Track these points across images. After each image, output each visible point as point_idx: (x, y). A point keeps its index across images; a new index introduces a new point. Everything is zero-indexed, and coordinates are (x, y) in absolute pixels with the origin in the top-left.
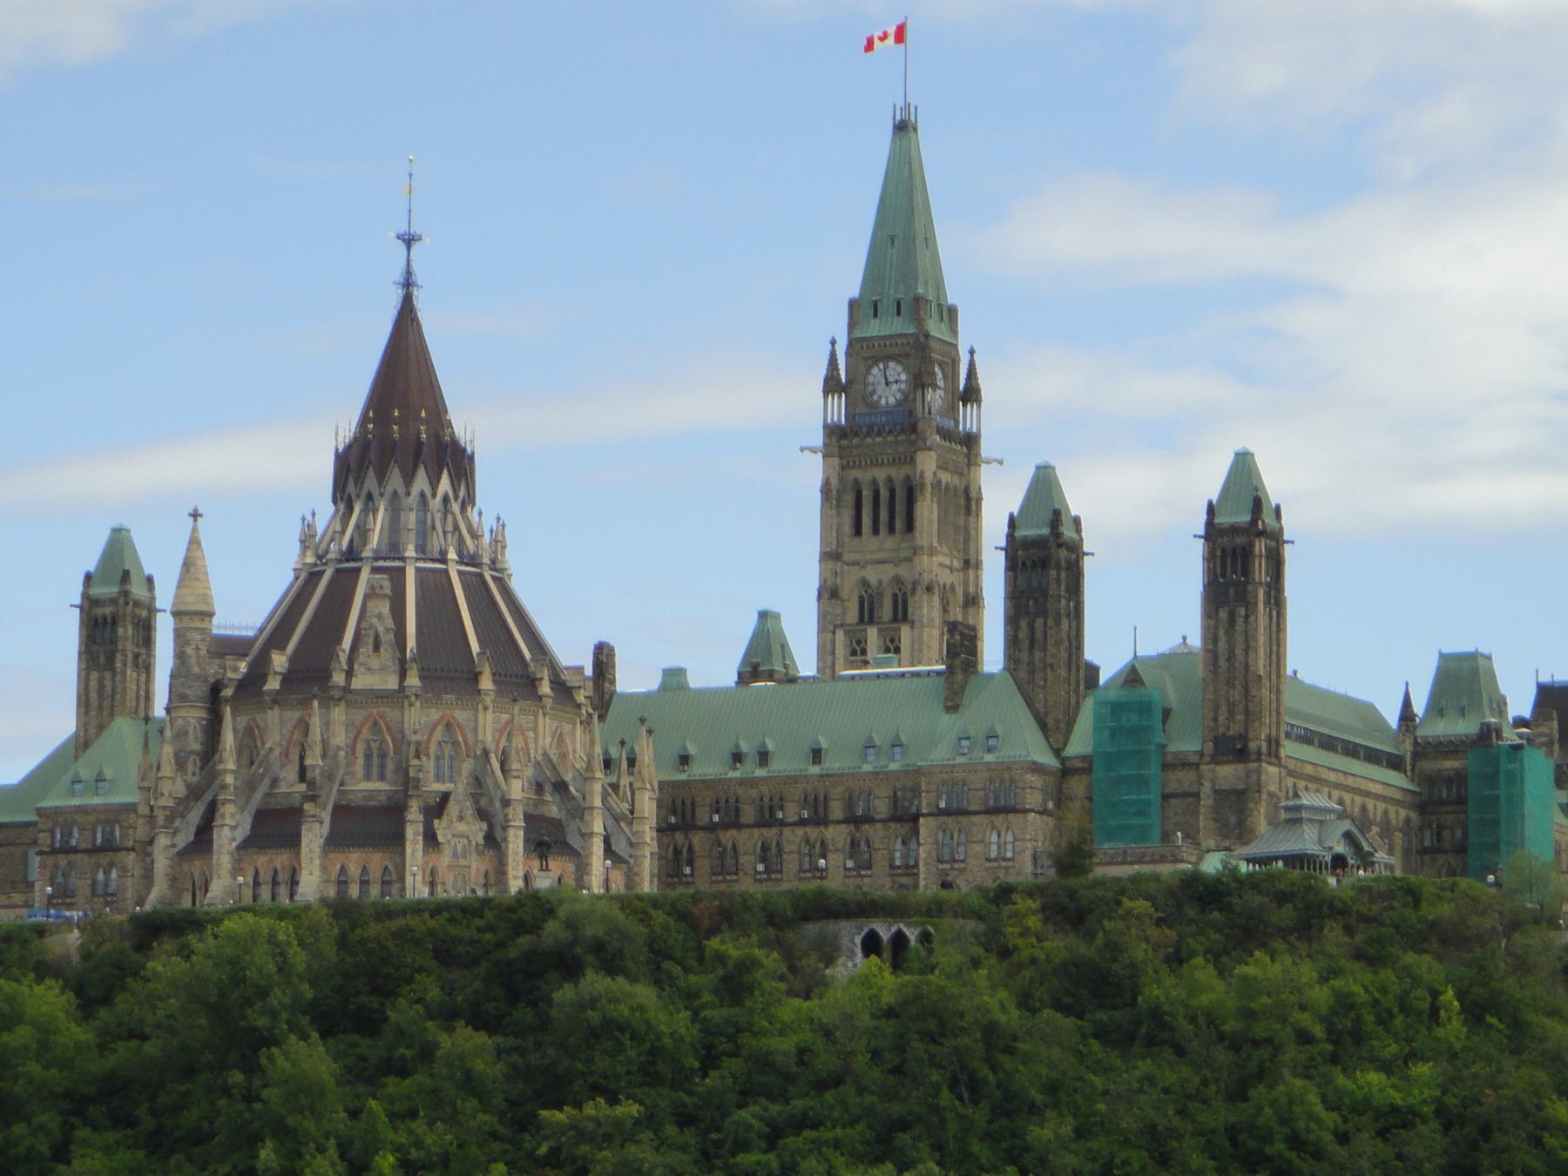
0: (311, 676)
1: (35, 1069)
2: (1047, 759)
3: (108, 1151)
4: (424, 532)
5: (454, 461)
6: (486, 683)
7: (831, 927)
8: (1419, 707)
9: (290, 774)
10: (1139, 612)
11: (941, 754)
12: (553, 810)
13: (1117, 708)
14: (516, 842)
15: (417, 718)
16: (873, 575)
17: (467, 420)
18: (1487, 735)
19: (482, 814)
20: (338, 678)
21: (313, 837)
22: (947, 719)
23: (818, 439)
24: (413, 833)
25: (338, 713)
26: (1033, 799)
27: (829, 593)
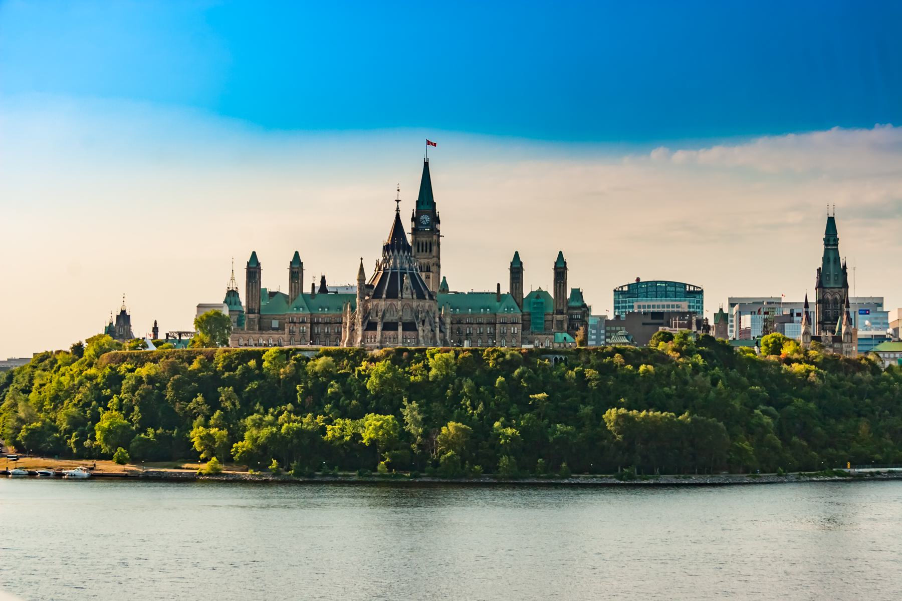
16: (423, 261)
21: (400, 328)
22: (498, 304)
25: (399, 303)
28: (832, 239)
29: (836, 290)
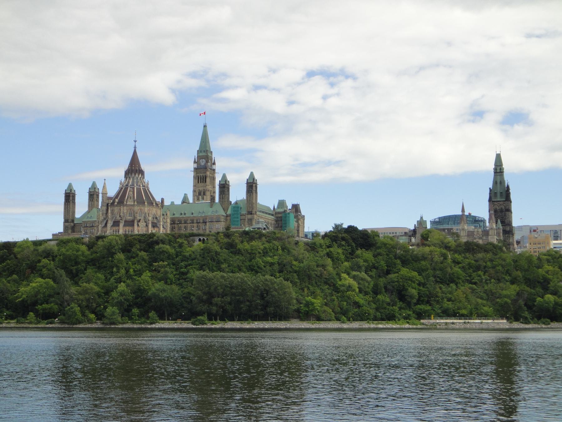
0: (121, 202)
1: (82, 258)
2: (225, 214)
3: (92, 269)
4: (137, 182)
5: (141, 172)
6: (146, 204)
7: (194, 238)
8: (276, 207)
9: (118, 216)
10: (237, 194)
11: (209, 214)
12: (155, 221)
13: (234, 207)
14: (150, 226)
15: (136, 208)
16: (200, 189)
17: (143, 167)
18: (285, 211)
19: (145, 222)
20: (125, 203)
21: (121, 225)
23: (193, 170)
24: (136, 224)
25: (125, 208)
26: (222, 220)
27: (194, 191)
28: (498, 168)
29: (501, 203)
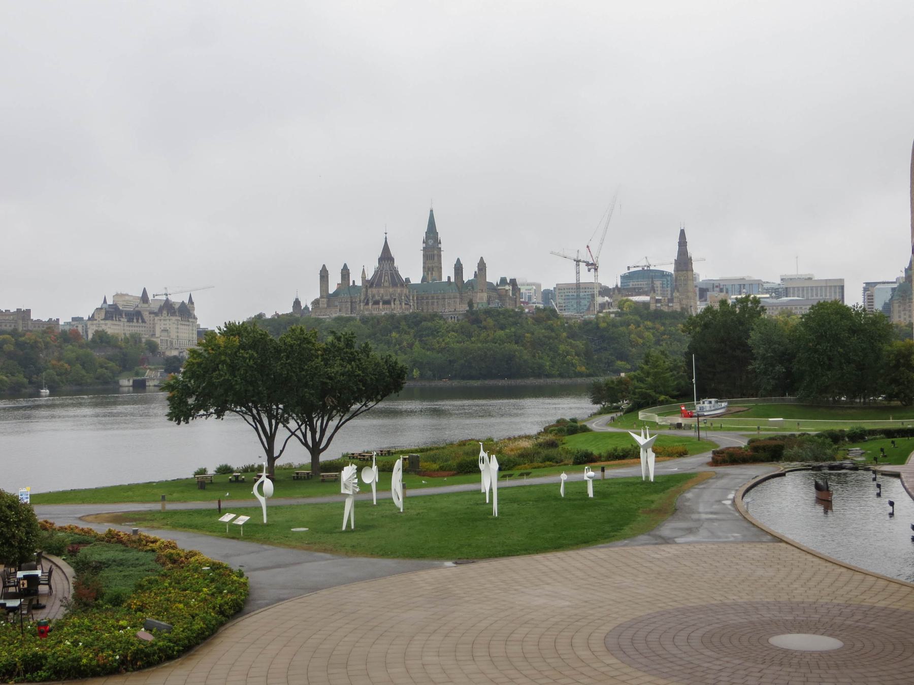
5: (392, 260)
27: (424, 267)
